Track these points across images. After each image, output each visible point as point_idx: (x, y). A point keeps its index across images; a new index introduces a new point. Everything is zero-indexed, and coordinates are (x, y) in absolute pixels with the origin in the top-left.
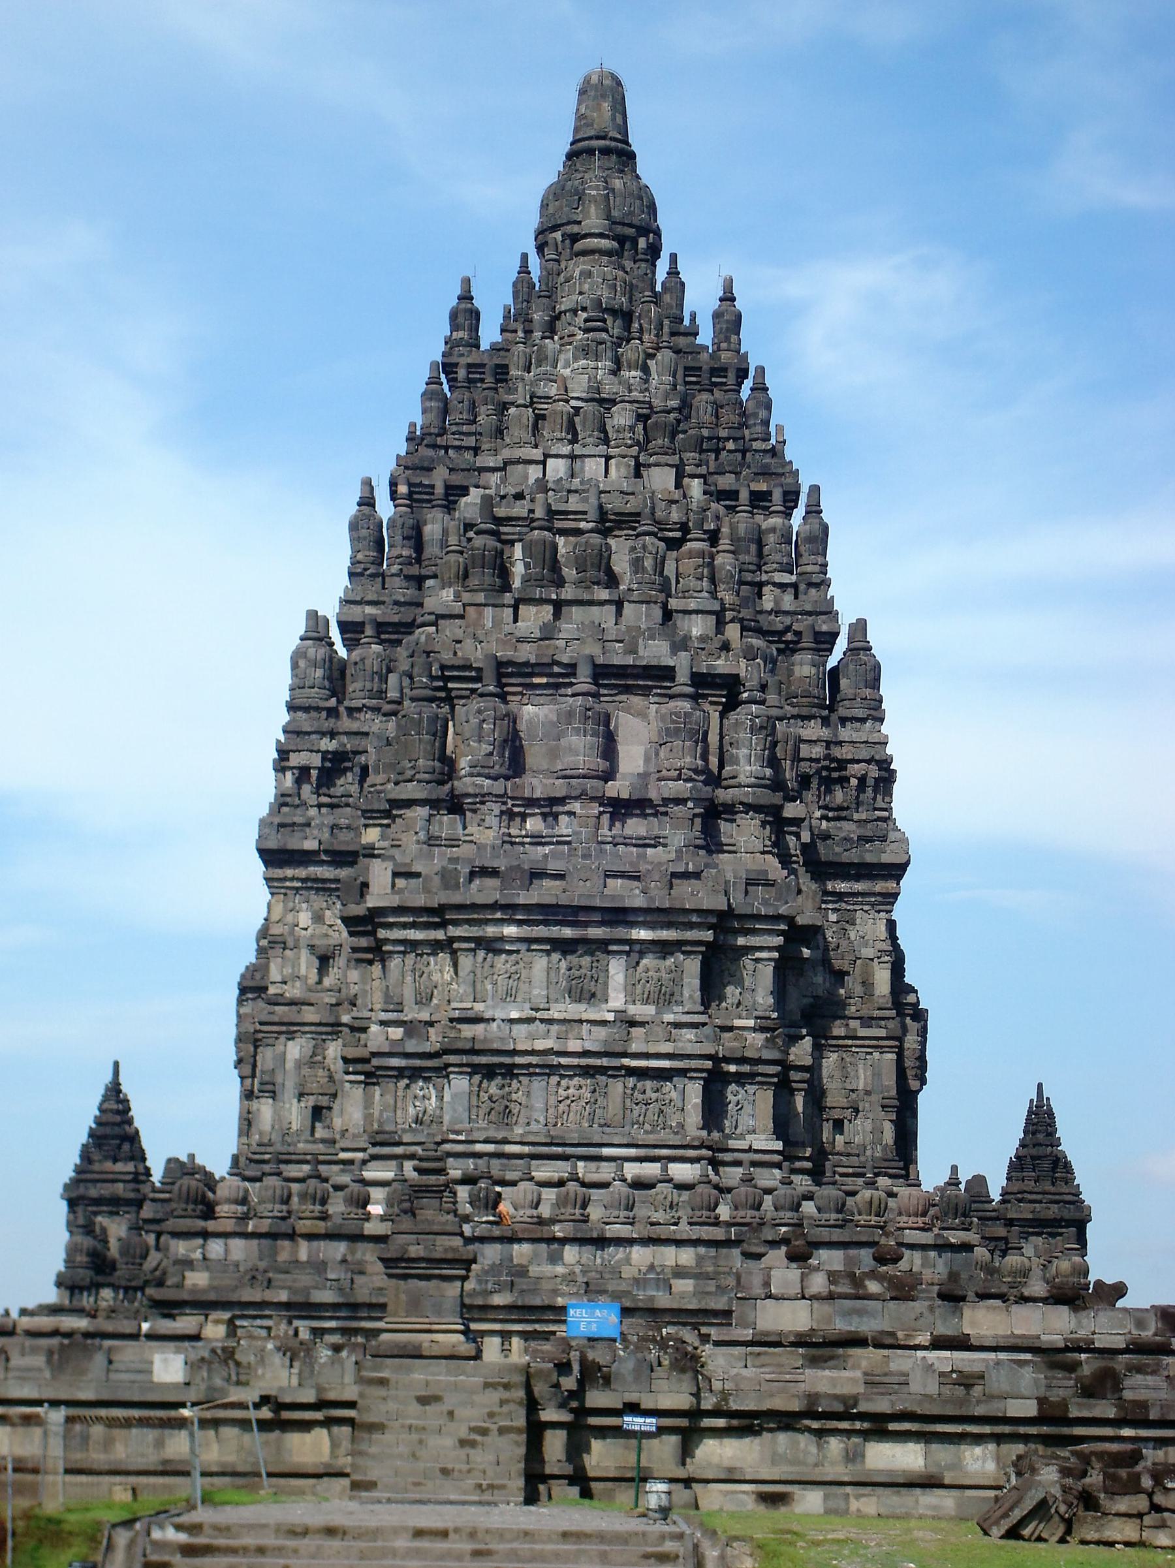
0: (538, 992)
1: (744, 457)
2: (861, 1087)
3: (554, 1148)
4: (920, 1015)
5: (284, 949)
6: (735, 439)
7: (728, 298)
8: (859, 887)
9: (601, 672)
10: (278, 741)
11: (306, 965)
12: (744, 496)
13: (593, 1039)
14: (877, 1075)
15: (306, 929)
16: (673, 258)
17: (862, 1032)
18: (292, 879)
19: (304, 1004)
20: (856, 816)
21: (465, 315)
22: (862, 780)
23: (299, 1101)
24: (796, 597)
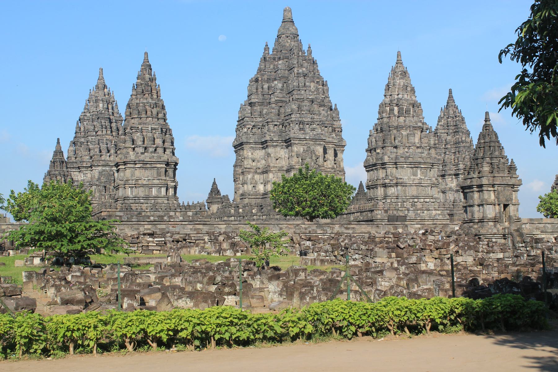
0: (409, 175)
3: (414, 197)
7: (309, 47)
9: (414, 127)
11: (250, 161)
13: (416, 181)
21: (267, 48)
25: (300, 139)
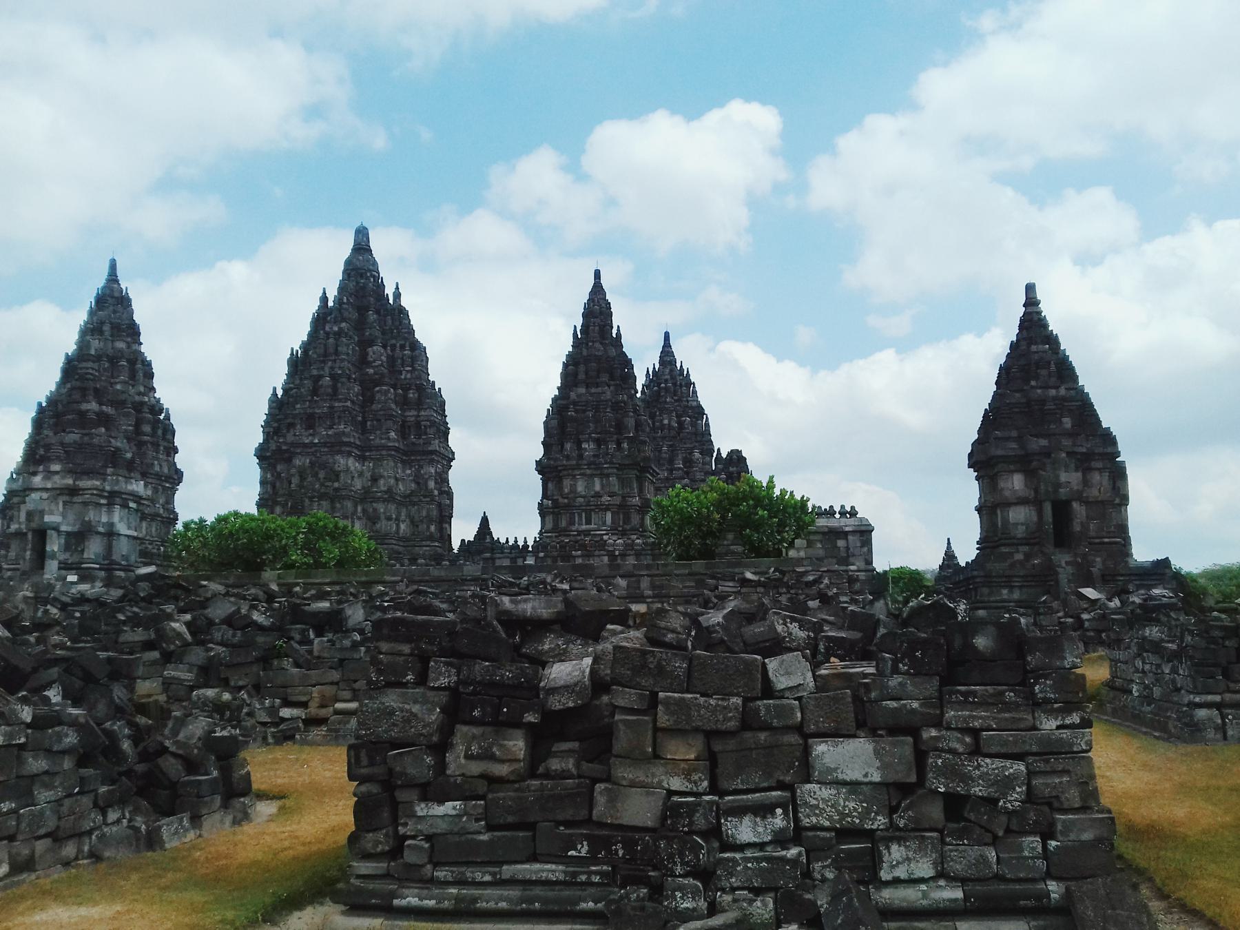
7: (397, 288)
14: (428, 510)
21: (324, 299)
25: (305, 445)
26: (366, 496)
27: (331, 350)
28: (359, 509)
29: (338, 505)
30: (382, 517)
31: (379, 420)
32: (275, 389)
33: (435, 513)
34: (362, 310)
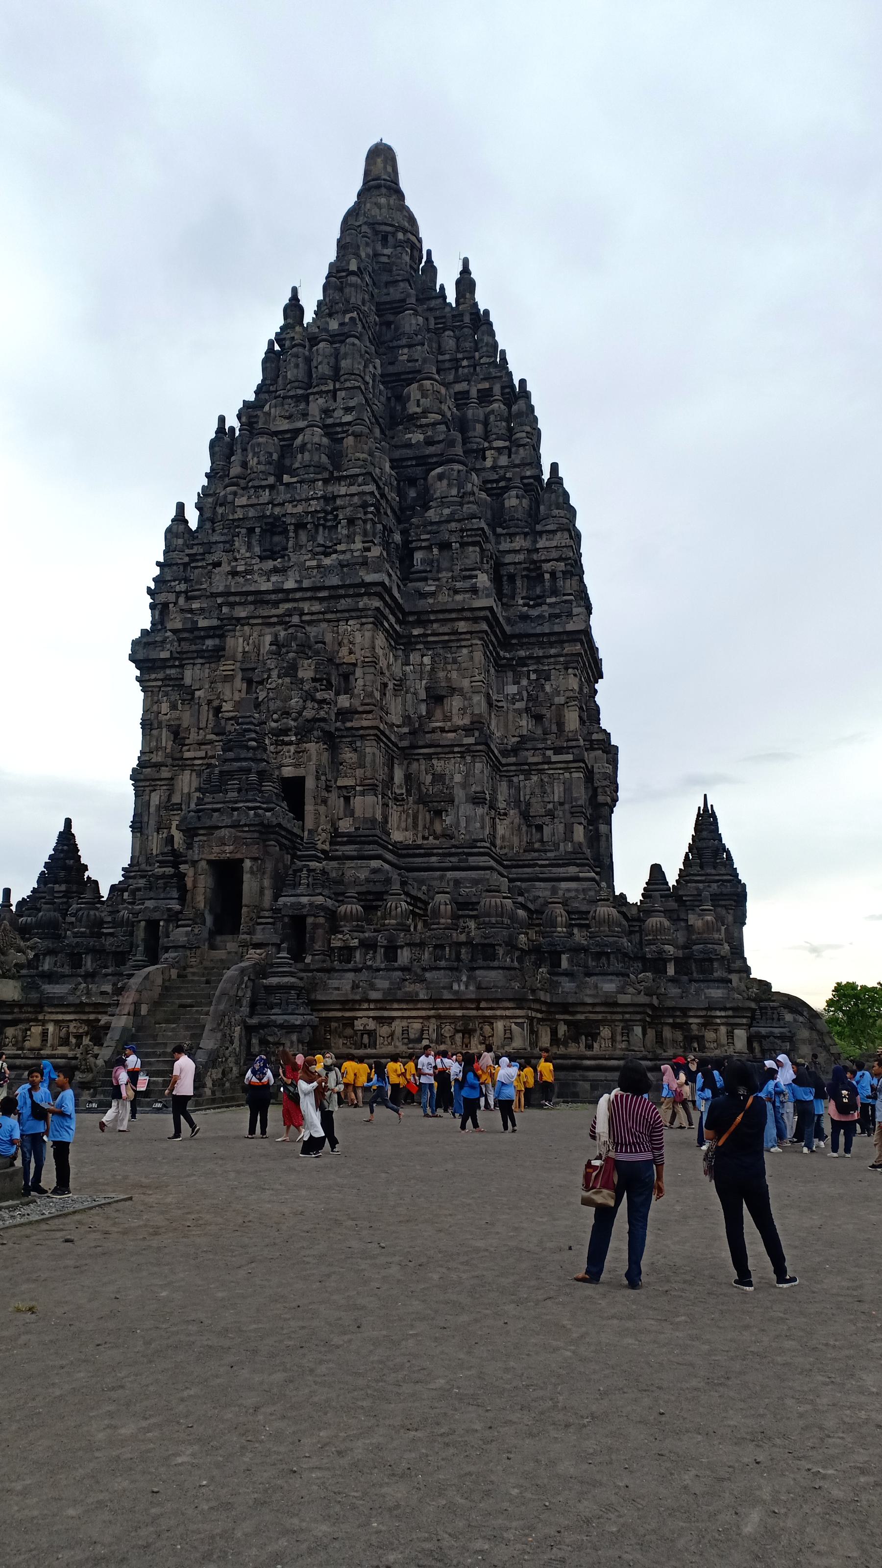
1: (475, 369)
2: (556, 800)
4: (611, 753)
5: (151, 730)
6: (467, 358)
7: (466, 271)
8: (553, 651)
10: (149, 588)
12: (474, 393)
14: (568, 790)
15: (166, 715)
16: (429, 252)
17: (554, 758)
18: (156, 680)
19: (162, 766)
20: (548, 600)
21: (293, 308)
22: (553, 574)
23: (158, 833)
24: (509, 457)
26: (410, 746)
27: (325, 369)
28: (399, 775)
29: (348, 756)
30: (459, 794)
31: (445, 546)
32: (181, 507)
33: (581, 794)
34: (390, 311)
